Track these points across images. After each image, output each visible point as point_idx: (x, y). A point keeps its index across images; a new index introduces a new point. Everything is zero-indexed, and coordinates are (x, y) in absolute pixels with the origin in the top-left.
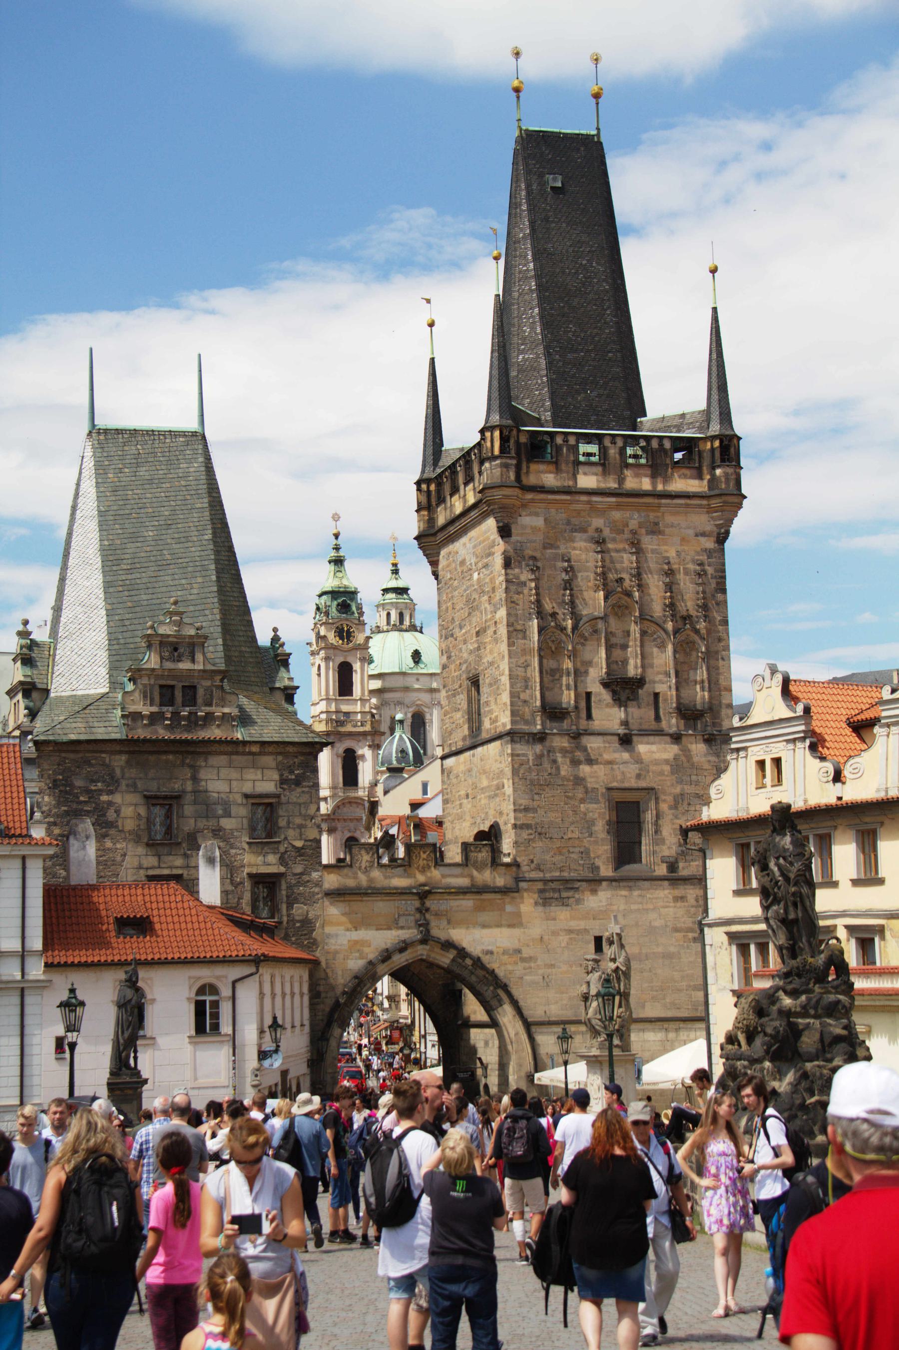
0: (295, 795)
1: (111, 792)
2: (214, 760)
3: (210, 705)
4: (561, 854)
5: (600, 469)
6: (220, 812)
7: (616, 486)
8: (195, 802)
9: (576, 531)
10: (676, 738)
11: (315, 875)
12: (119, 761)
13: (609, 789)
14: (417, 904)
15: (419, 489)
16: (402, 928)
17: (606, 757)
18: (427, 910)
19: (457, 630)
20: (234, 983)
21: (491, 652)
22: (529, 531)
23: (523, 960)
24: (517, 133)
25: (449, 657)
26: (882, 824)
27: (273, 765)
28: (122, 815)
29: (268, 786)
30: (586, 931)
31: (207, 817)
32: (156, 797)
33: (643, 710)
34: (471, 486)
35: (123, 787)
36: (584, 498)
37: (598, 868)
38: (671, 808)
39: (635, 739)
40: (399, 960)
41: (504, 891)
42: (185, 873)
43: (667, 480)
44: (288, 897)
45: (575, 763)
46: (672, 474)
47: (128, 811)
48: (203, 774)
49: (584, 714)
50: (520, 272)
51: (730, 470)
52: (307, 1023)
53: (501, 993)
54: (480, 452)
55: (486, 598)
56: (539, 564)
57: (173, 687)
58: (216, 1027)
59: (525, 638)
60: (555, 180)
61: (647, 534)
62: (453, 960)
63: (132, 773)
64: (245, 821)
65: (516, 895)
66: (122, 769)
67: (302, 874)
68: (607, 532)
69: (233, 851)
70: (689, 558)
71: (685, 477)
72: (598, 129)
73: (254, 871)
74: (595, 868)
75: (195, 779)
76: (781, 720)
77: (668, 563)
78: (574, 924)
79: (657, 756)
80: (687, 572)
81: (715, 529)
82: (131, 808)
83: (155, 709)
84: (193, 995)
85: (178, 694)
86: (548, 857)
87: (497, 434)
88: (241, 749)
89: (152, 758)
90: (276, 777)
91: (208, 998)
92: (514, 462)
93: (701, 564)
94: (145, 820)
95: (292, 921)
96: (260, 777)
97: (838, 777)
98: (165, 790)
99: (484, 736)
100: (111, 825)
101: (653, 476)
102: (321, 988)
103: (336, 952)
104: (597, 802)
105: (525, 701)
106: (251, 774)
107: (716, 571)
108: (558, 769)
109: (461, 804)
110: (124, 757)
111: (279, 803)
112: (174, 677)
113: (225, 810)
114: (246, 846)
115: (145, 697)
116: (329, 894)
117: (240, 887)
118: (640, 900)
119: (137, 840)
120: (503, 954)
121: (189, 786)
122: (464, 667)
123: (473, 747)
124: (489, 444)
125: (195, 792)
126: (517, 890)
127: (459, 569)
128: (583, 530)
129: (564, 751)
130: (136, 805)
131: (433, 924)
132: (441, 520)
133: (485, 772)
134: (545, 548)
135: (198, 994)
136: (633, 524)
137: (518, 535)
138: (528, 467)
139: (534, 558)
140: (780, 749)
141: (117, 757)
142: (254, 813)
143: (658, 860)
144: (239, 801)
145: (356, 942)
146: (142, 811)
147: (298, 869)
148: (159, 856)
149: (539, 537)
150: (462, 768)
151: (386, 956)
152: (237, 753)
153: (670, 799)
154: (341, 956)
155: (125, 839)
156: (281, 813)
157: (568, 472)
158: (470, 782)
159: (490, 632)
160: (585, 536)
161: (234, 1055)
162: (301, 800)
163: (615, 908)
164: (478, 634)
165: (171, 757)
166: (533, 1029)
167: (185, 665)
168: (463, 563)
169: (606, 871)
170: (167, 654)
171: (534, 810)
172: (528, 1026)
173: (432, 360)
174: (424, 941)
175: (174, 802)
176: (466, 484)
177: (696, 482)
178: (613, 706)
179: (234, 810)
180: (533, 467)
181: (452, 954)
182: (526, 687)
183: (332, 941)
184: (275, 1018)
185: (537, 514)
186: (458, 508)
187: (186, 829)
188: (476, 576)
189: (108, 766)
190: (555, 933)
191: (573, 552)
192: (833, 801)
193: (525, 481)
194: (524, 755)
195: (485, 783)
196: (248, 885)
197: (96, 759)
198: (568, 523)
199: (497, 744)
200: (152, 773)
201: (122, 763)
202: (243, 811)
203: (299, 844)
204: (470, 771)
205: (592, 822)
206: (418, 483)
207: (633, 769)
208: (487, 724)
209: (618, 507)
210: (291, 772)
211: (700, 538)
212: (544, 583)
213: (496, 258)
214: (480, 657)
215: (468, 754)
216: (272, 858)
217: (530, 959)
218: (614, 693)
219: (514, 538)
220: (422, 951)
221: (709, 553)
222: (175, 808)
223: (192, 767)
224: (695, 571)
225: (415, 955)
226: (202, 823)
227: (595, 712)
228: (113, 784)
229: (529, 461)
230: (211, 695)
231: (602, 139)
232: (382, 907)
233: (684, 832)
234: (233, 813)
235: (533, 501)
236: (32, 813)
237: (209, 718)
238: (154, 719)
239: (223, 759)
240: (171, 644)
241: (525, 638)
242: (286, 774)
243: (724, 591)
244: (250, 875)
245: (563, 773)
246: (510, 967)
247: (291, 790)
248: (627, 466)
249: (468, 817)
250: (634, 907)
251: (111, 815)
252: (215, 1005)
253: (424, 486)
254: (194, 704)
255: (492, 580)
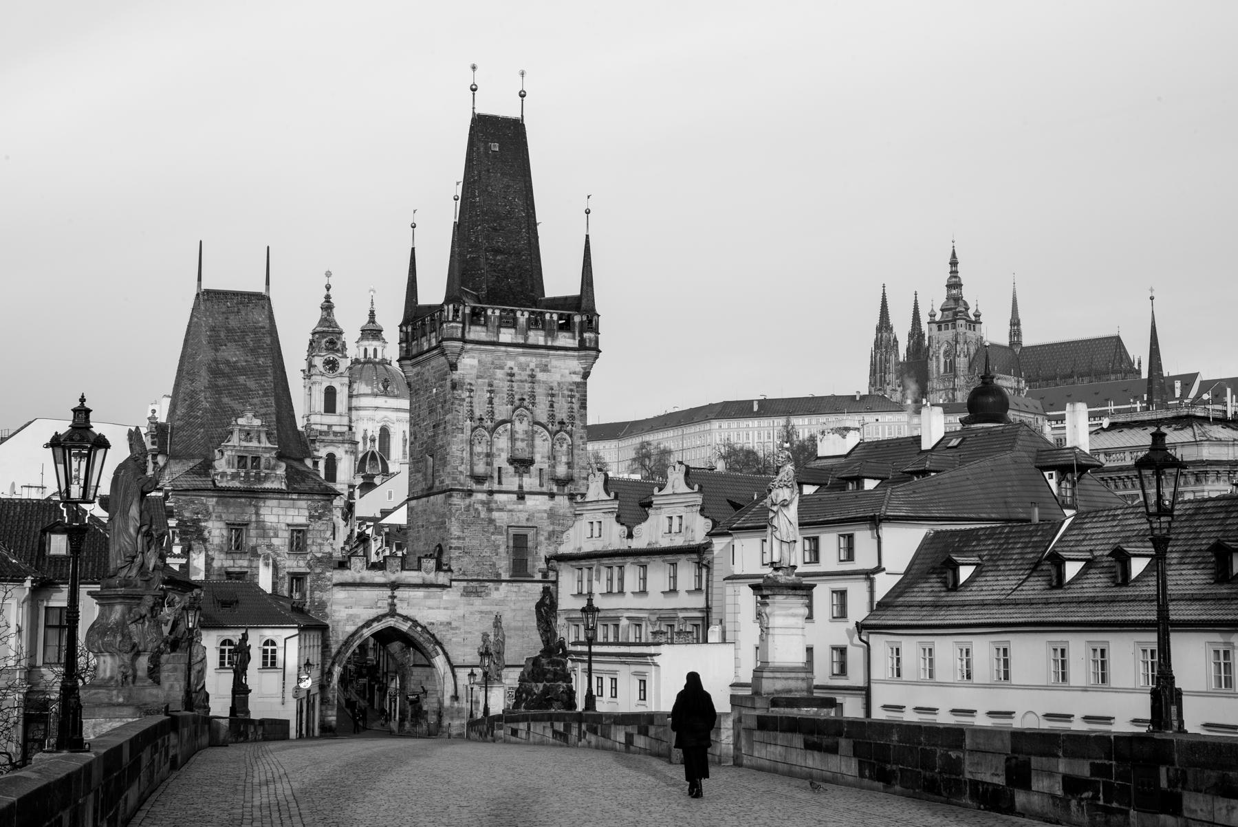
0: (318, 525)
1: (206, 521)
2: (269, 503)
3: (268, 469)
4: (478, 565)
5: (513, 331)
6: (272, 534)
7: (523, 342)
8: (257, 528)
9: (497, 368)
10: (552, 496)
11: (328, 574)
12: (211, 502)
13: (508, 526)
14: (389, 593)
15: (401, 331)
16: (380, 607)
17: (509, 507)
18: (395, 597)
19: (421, 422)
20: (286, 639)
21: (442, 440)
22: (468, 367)
23: (452, 629)
24: (470, 117)
25: (415, 438)
26: (649, 563)
27: (306, 506)
28: (212, 534)
29: (302, 519)
30: (491, 612)
31: (264, 537)
32: (234, 524)
33: (532, 479)
34: (434, 333)
35: (214, 518)
36: (503, 348)
37: (500, 574)
38: (546, 539)
39: (526, 496)
40: (377, 627)
41: (443, 586)
42: (249, 570)
43: (554, 339)
44: (311, 587)
45: (490, 510)
46: (557, 335)
47: (216, 532)
48: (262, 511)
49: (496, 480)
50: (471, 202)
51: (592, 335)
52: (320, 663)
53: (438, 648)
54: (441, 315)
55: (440, 405)
56: (473, 388)
57: (246, 457)
58: (273, 664)
59: (463, 433)
60: (495, 146)
61: (541, 371)
62: (410, 628)
63: (219, 509)
64: (287, 540)
65: (449, 589)
66: (213, 506)
67: (321, 573)
68: (516, 370)
69: (279, 559)
70: (565, 387)
71: (565, 337)
72: (522, 116)
73: (291, 570)
74: (499, 575)
75: (257, 514)
76: (602, 501)
77: (552, 389)
78: (484, 608)
79: (539, 508)
80: (563, 397)
81: (582, 371)
82: (218, 531)
83: (234, 470)
84: (262, 645)
85: (249, 462)
86: (470, 567)
87: (451, 307)
88: (286, 496)
89: (232, 500)
90: (307, 514)
91: (270, 648)
92: (461, 325)
93: (571, 390)
94: (225, 538)
95: (312, 602)
96: (297, 514)
97: (630, 536)
98: (239, 520)
99: (435, 490)
100: (205, 540)
101: (545, 337)
102: (327, 642)
103: (339, 621)
104: (502, 534)
105: (461, 472)
106: (291, 512)
107: (581, 395)
108: (479, 513)
109: (418, 531)
110: (215, 499)
111: (308, 530)
112: (247, 451)
113: (275, 533)
114: (287, 555)
115: (229, 463)
116: (336, 585)
117: (282, 580)
118: (525, 594)
119: (221, 550)
120: (441, 625)
121: (254, 518)
122: (425, 446)
123: (428, 495)
124: (446, 314)
125: (257, 522)
126: (450, 587)
127: (425, 385)
128: (502, 368)
129: (483, 503)
130: (221, 529)
131: (398, 606)
132: (414, 352)
133: (433, 512)
134: (477, 378)
135: (265, 644)
136: (532, 365)
137: (462, 369)
138: (470, 328)
139: (471, 384)
140: (599, 516)
141: (211, 499)
142: (292, 537)
143: (536, 570)
144: (284, 528)
145: (351, 615)
146: (225, 533)
147: (318, 570)
148: (234, 560)
149: (474, 372)
150: (420, 508)
151: (368, 624)
152: (284, 499)
153: (546, 534)
154: (342, 623)
155: (214, 549)
156: (309, 536)
157: (494, 332)
158: (425, 517)
159: (442, 427)
160: (502, 371)
161: (284, 679)
162: (322, 528)
163: (509, 599)
164: (434, 427)
165: (243, 500)
166: (456, 670)
167: (254, 444)
168: (427, 381)
169: (505, 576)
170: (243, 437)
171: (464, 539)
172: (453, 667)
173: (413, 249)
174: (393, 616)
175: (244, 528)
176: (431, 332)
177: (572, 341)
178: (515, 476)
179: (280, 534)
180: (473, 328)
181: (410, 623)
182: (462, 463)
183: (337, 614)
184: (308, 660)
185: (474, 357)
186: (426, 347)
187: (251, 544)
188: (434, 390)
189: (205, 504)
190: (471, 613)
191: (495, 382)
192: (626, 548)
193: (468, 337)
194: (458, 505)
195: (434, 519)
196: (287, 579)
197: (198, 500)
198: (493, 363)
199: (442, 496)
200: (231, 510)
201: (214, 503)
202: (287, 535)
203: (319, 555)
204: (425, 510)
205: (498, 547)
206: (401, 326)
207: (524, 516)
208: (437, 483)
209: (524, 354)
210: (316, 511)
211: (572, 375)
212: (475, 400)
213: (455, 199)
214: (434, 441)
215: (425, 499)
216: (302, 563)
217: (456, 628)
218: (515, 467)
219: (459, 372)
220: (390, 622)
221: (577, 384)
222: (244, 531)
223: (254, 506)
224: (568, 396)
225: (386, 624)
226: (260, 541)
227: (504, 480)
228: (208, 515)
229: (473, 323)
230: (269, 463)
231: (525, 123)
232: (367, 594)
233: (548, 560)
234: (280, 535)
235: (471, 349)
236: (174, 539)
237: (267, 477)
238: (234, 476)
239: (275, 502)
240: (246, 431)
241: (463, 433)
242: (313, 512)
243: (585, 408)
244: (288, 573)
245: (482, 516)
246: (444, 633)
247: (315, 522)
248: (530, 329)
249: (423, 539)
250: (520, 599)
251: (206, 533)
252: (274, 651)
253: (404, 328)
254: (259, 468)
255: (445, 395)
